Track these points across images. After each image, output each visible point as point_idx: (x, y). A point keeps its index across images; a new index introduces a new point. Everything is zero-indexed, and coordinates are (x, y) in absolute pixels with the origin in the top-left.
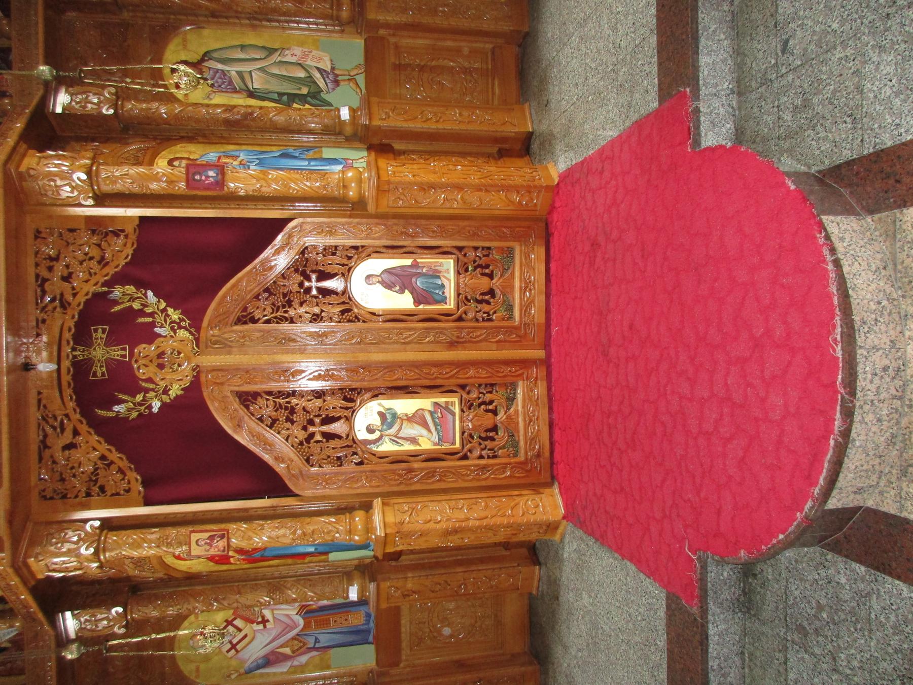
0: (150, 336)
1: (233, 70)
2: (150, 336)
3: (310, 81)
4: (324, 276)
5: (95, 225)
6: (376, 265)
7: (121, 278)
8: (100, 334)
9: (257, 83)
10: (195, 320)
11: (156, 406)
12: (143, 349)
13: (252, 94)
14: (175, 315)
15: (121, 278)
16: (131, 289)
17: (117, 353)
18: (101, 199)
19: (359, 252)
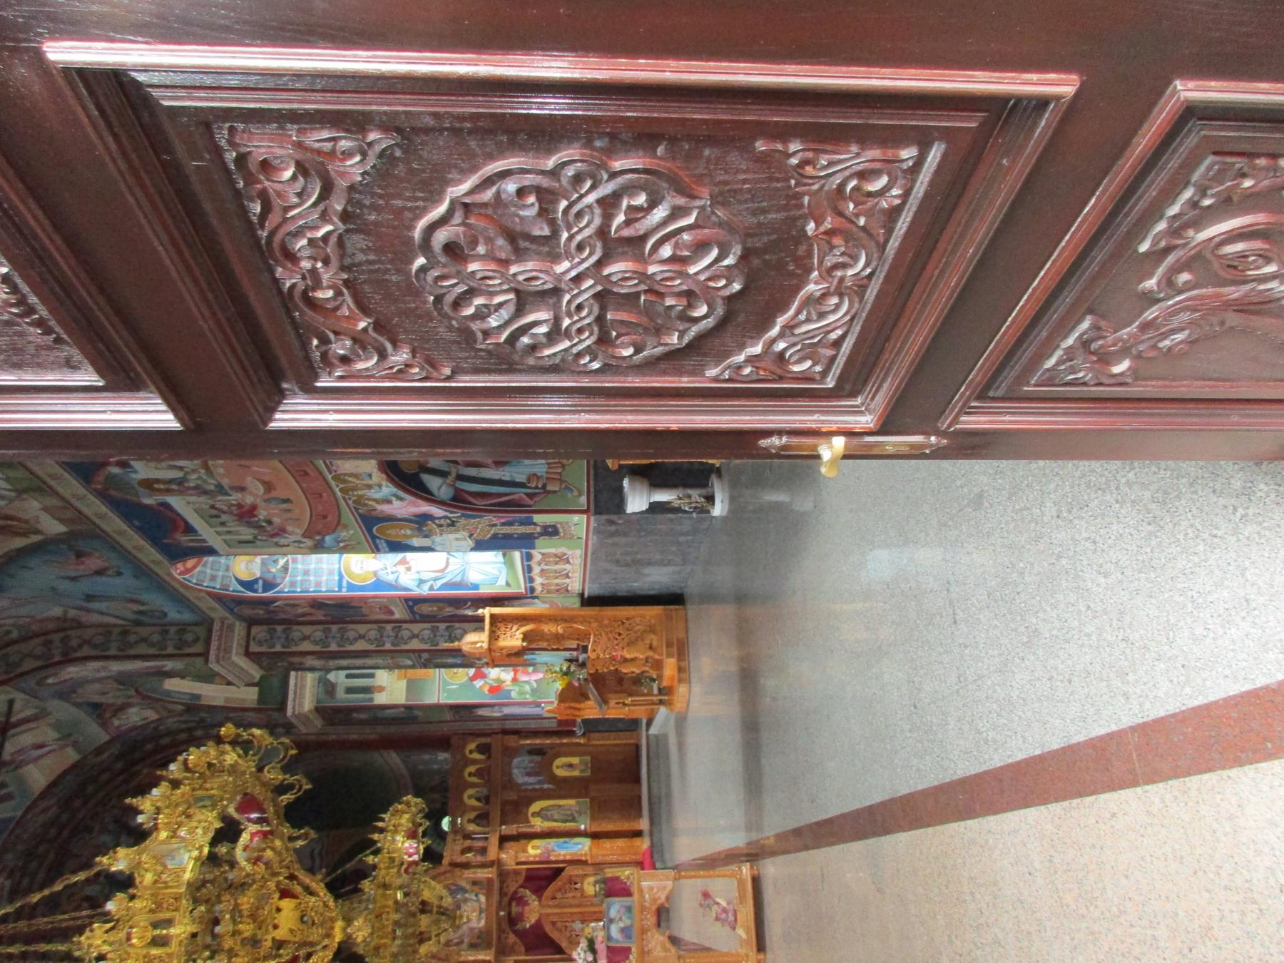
0: (528, 904)
1: (549, 813)
2: (528, 904)
3: (572, 815)
4: (576, 883)
5: (516, 873)
6: (591, 879)
7: (521, 886)
8: (514, 904)
9: (556, 817)
10: (540, 897)
11: (528, 926)
12: (527, 908)
13: (556, 821)
14: (534, 897)
15: (521, 886)
16: (522, 889)
17: (519, 909)
18: (518, 864)
19: (586, 875)
